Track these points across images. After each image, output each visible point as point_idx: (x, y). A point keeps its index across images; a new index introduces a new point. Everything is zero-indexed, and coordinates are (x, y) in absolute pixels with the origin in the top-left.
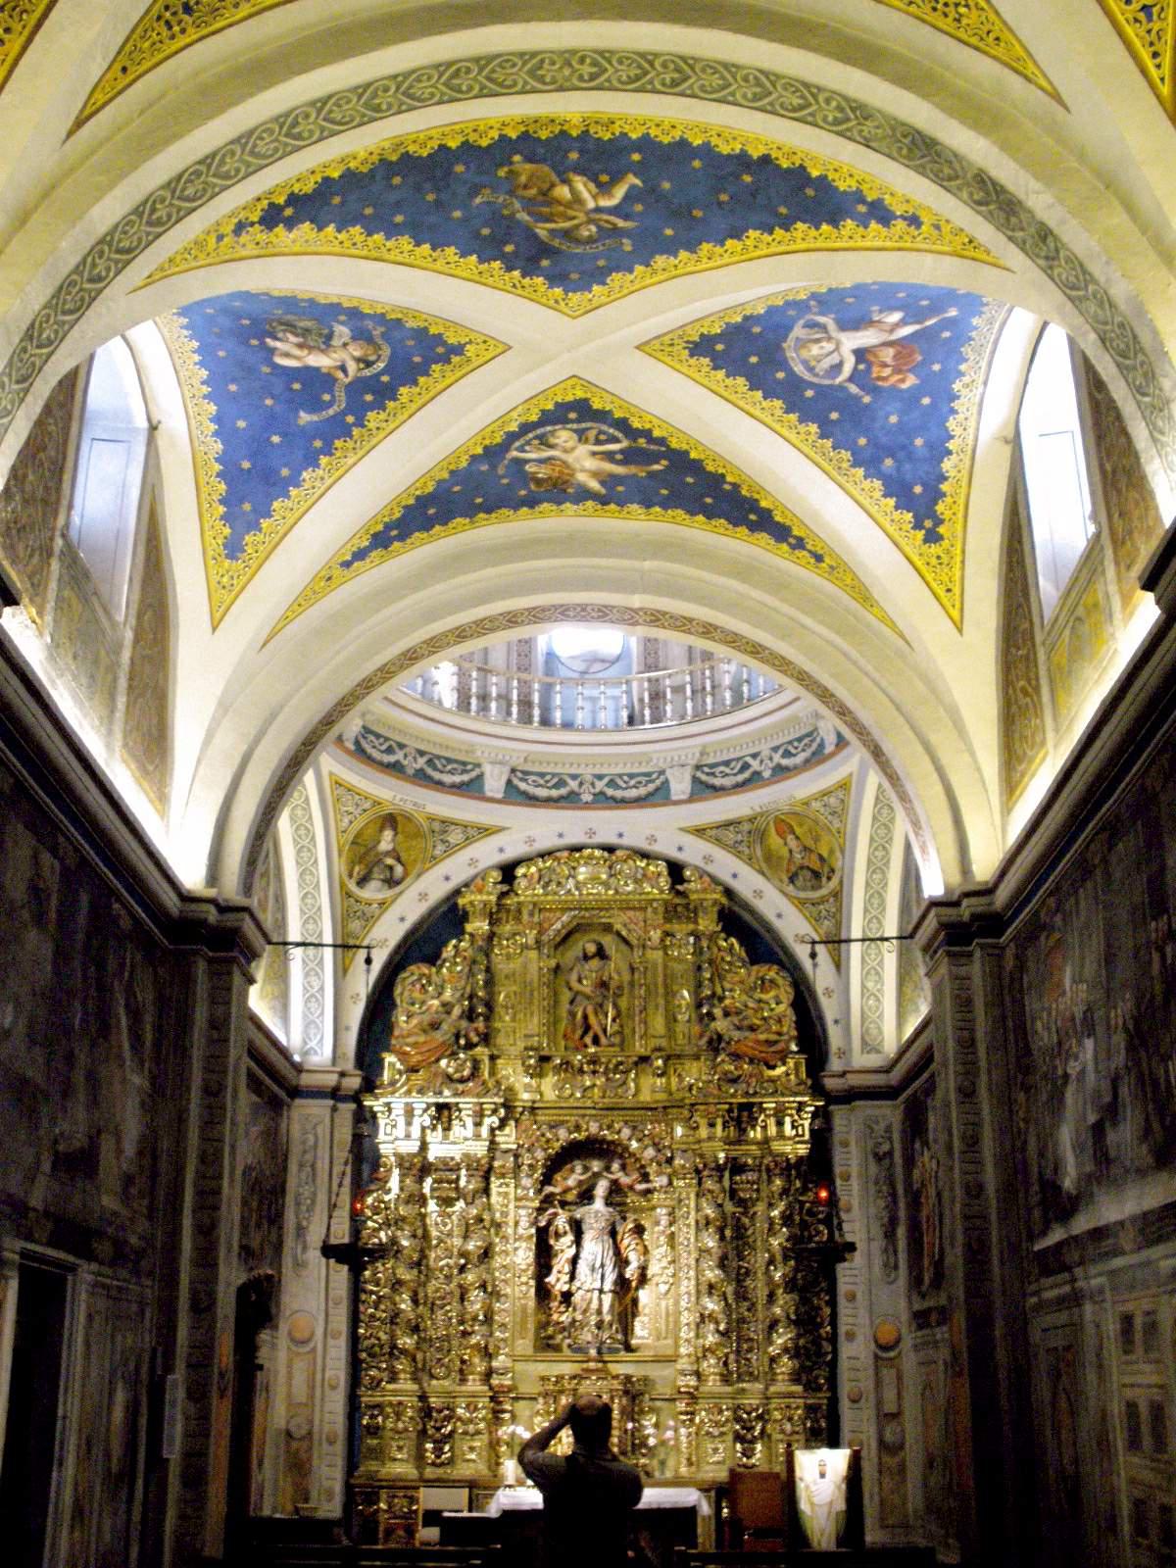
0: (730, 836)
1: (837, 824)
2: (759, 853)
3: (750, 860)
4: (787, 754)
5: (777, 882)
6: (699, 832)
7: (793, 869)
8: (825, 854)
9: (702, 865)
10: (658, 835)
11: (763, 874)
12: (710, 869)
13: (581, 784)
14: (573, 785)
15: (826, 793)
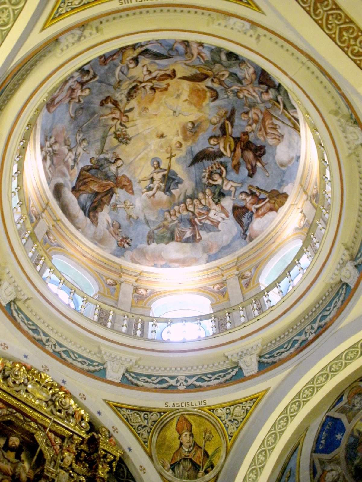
0: (138, 420)
1: (232, 429)
2: (154, 440)
3: (144, 443)
4: (200, 379)
5: (160, 466)
6: (117, 408)
7: (178, 459)
8: (210, 453)
9: (111, 430)
10: (87, 396)
11: (151, 457)
12: (115, 434)
13: (48, 341)
14: (44, 339)
15: (234, 404)
